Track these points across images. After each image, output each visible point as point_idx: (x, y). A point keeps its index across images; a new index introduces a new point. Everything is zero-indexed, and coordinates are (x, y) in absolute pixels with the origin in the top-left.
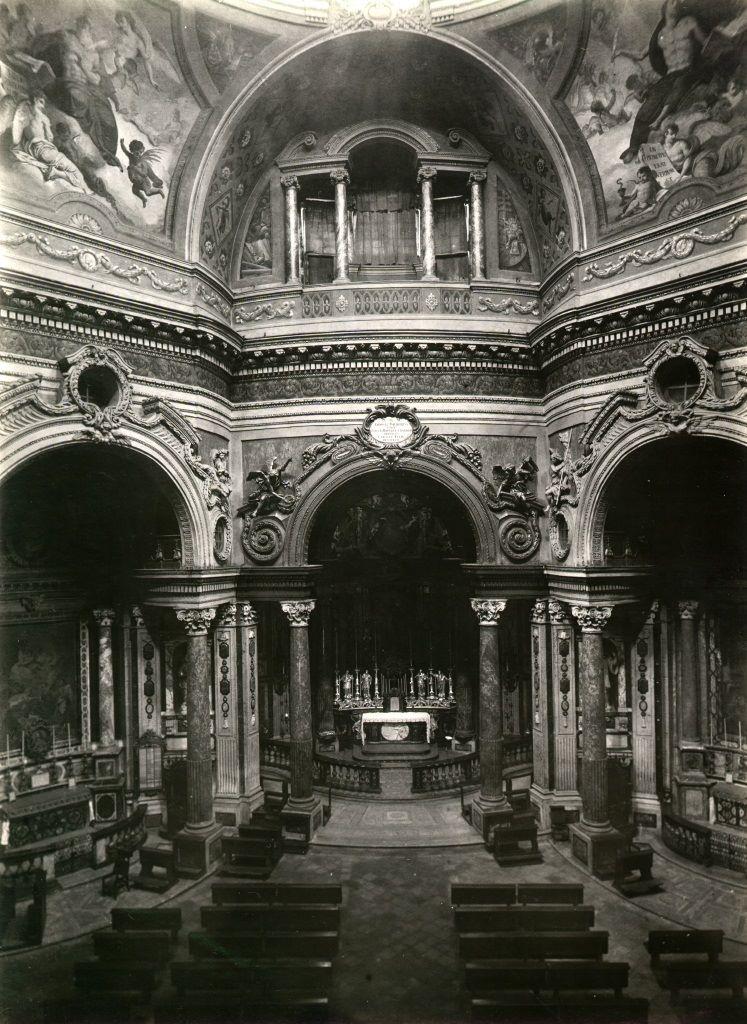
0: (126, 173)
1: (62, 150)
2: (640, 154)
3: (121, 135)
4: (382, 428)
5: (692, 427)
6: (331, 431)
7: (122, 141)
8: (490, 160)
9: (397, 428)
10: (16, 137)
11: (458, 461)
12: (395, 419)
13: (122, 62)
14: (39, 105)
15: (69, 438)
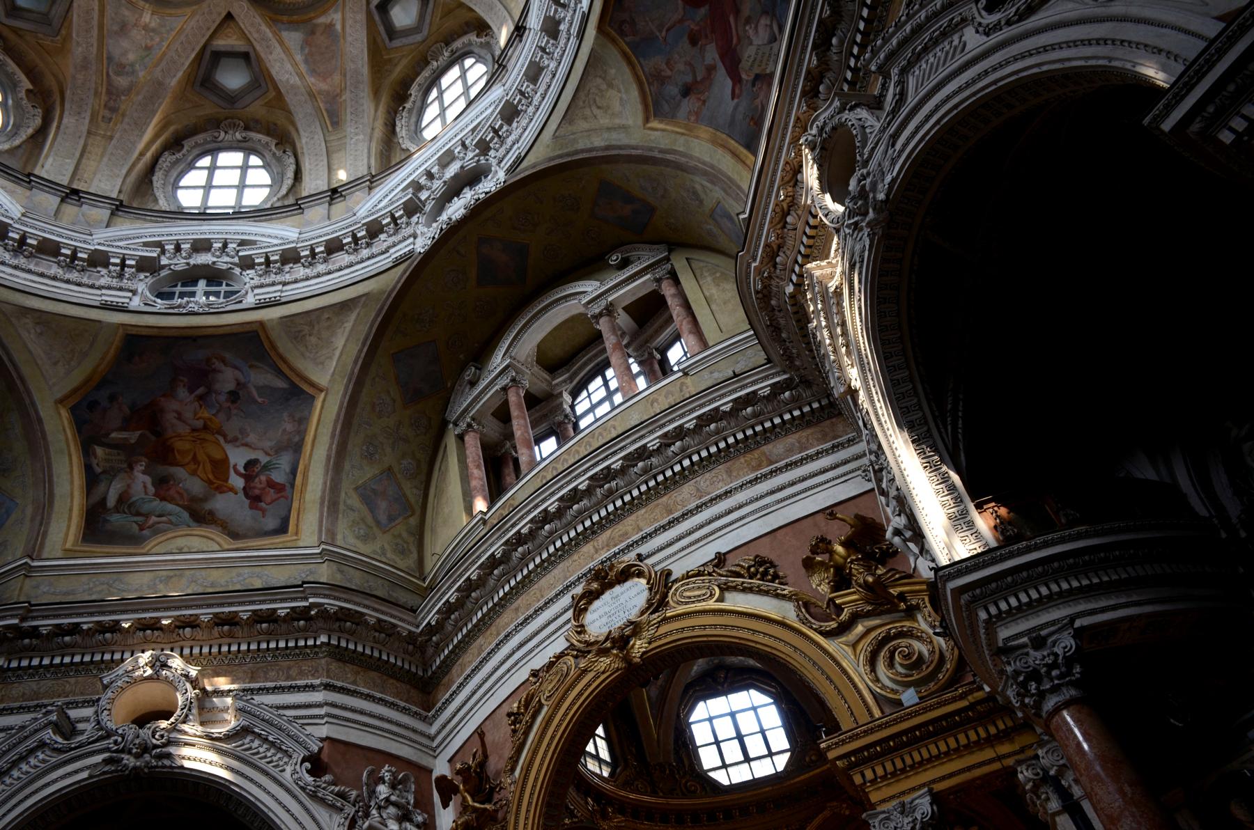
0: (241, 495)
1: (163, 499)
2: (744, 76)
3: (232, 461)
4: (601, 612)
5: (880, 186)
6: (539, 662)
7: (235, 466)
8: (670, 251)
9: (622, 600)
10: (111, 502)
11: (735, 589)
12: (617, 589)
13: (222, 398)
14: (140, 467)
15: (85, 775)
